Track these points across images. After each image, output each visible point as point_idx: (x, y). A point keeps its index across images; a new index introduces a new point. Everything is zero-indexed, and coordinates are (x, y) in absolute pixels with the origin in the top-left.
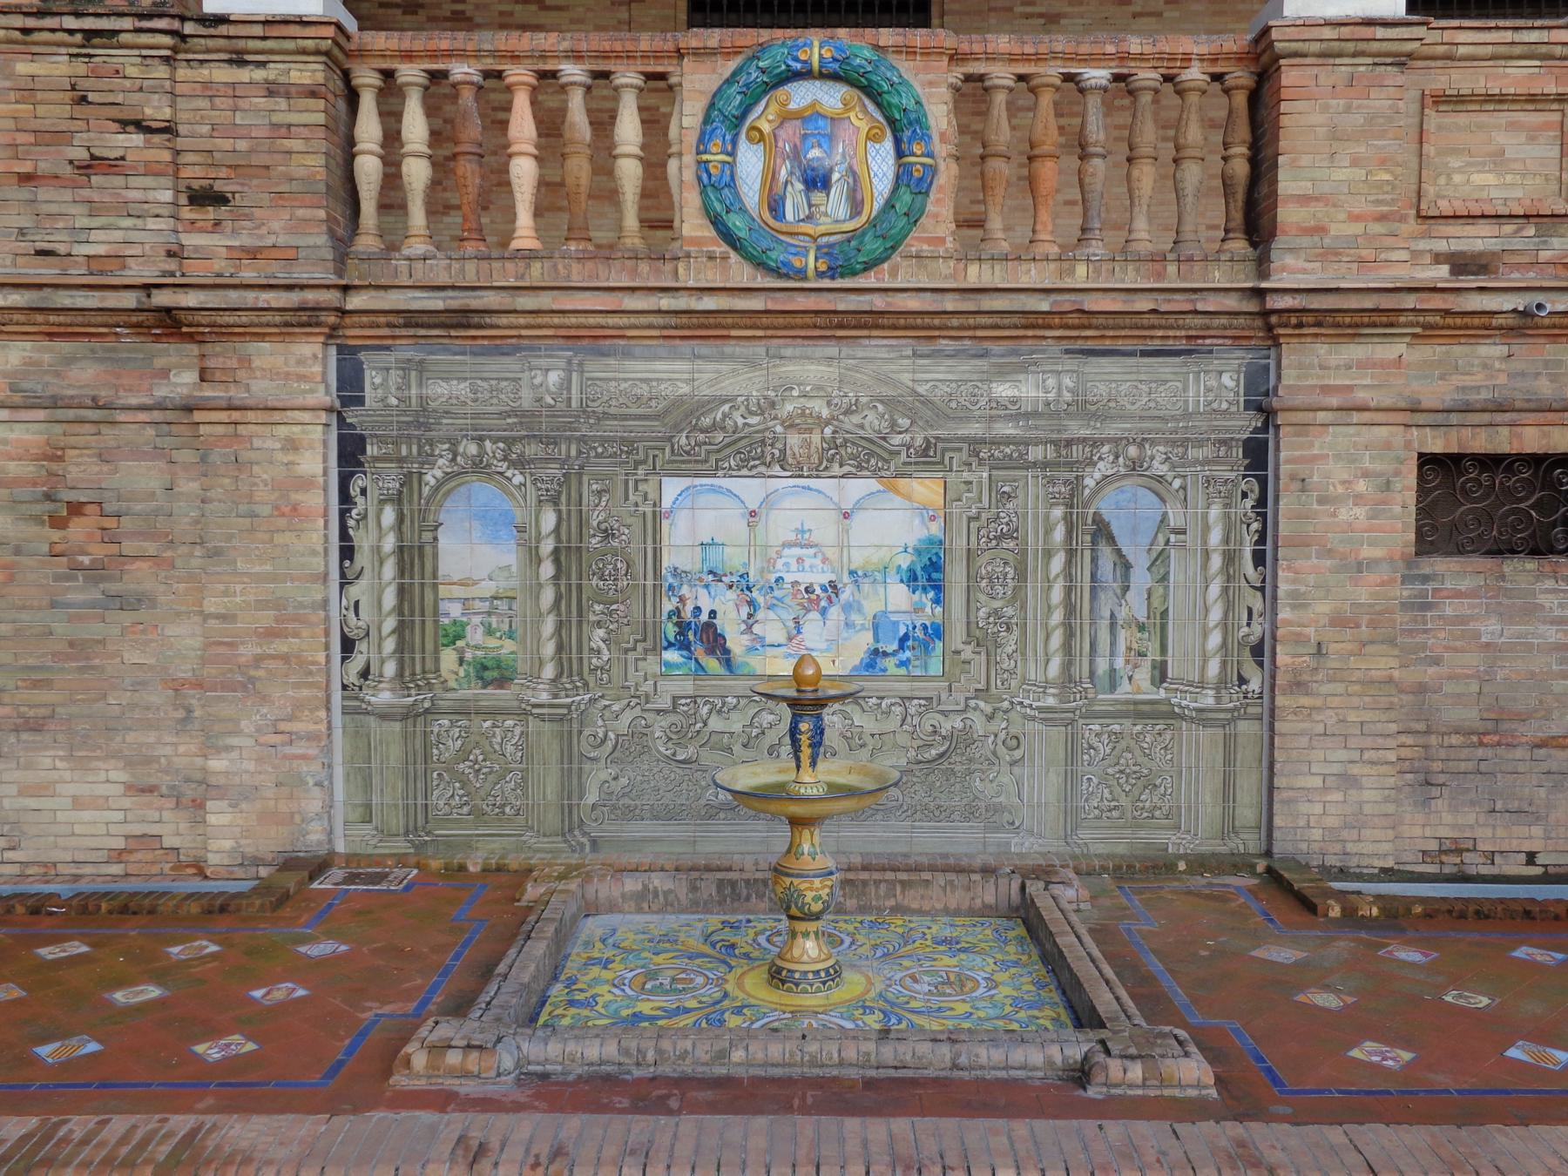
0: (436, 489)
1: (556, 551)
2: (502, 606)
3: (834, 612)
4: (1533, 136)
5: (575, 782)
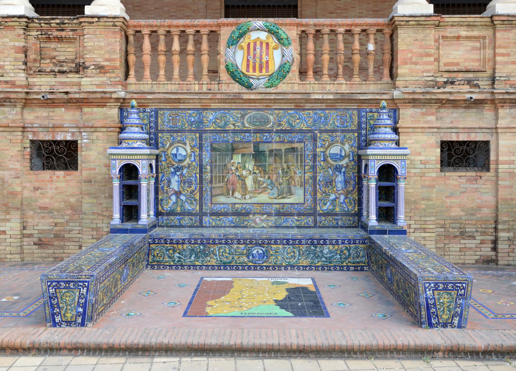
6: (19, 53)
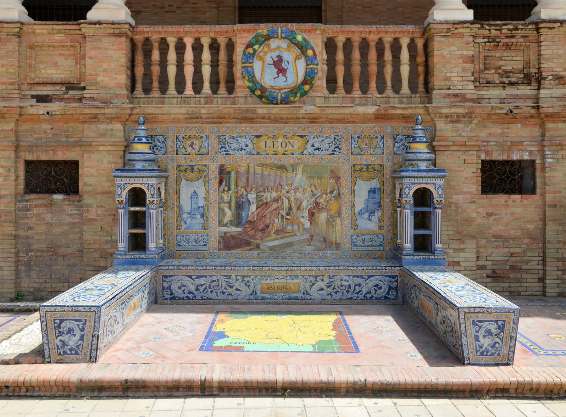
4: (67, 57)
6: (467, 62)
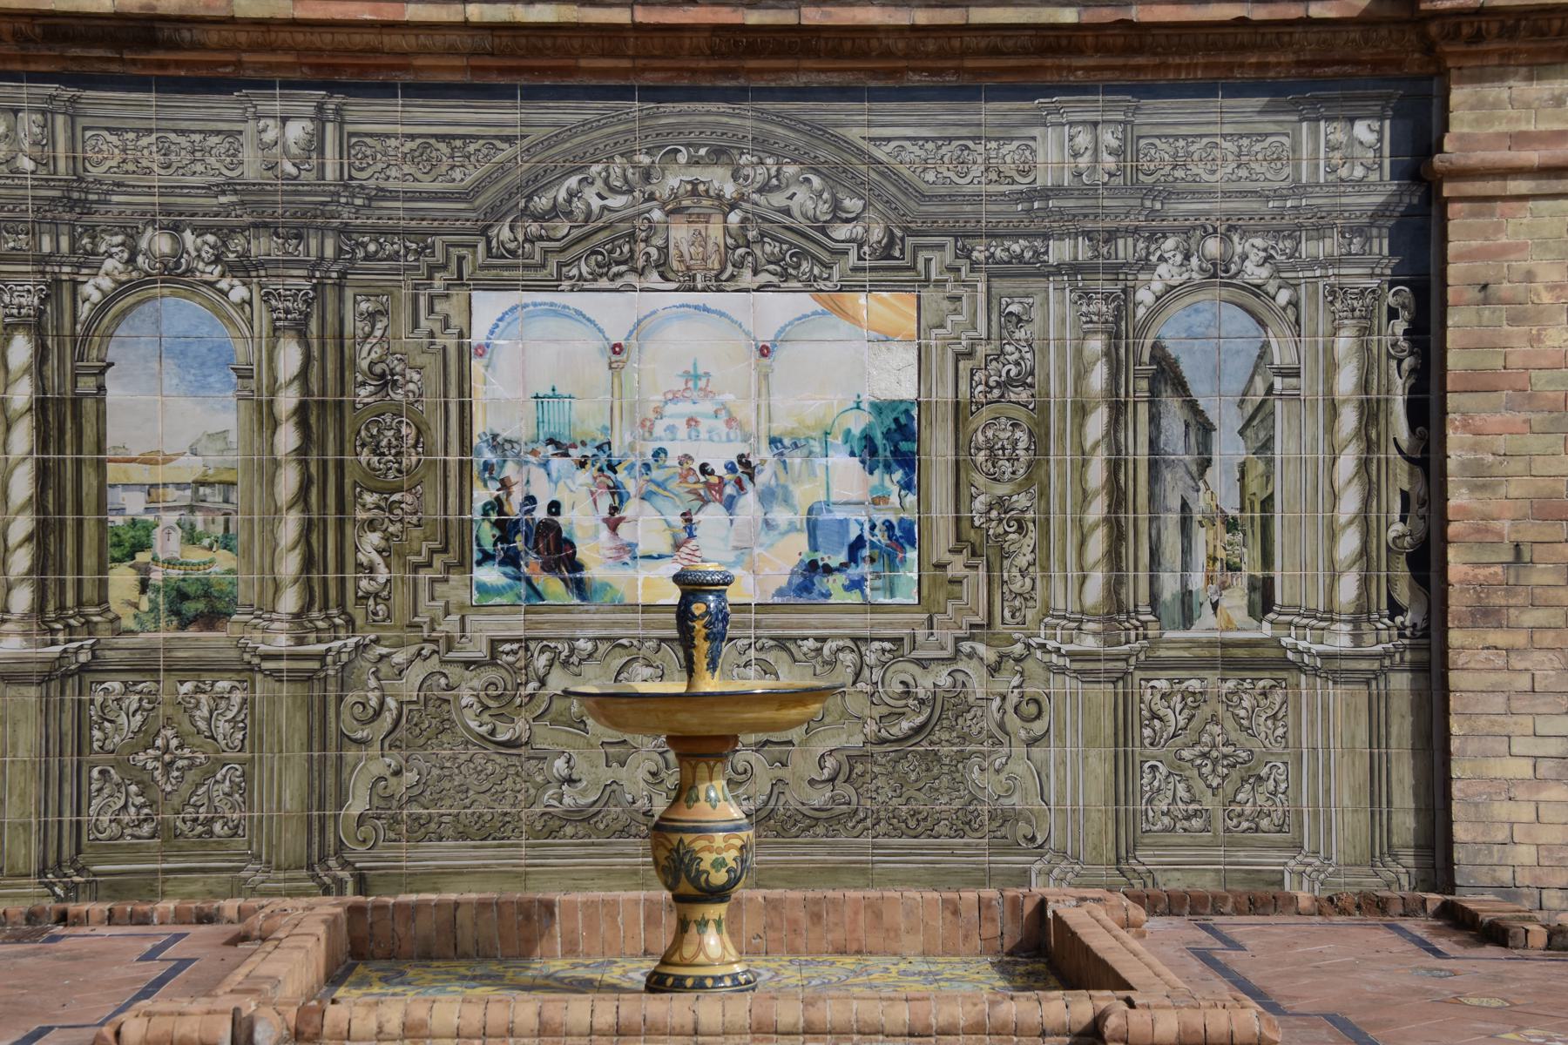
0: (102, 309)
1: (302, 411)
2: (214, 497)
3: (749, 502)
5: (331, 779)
